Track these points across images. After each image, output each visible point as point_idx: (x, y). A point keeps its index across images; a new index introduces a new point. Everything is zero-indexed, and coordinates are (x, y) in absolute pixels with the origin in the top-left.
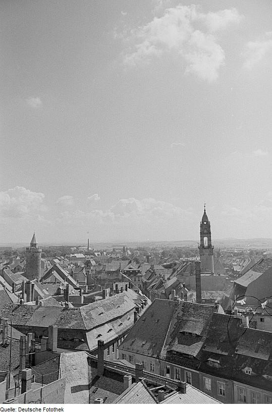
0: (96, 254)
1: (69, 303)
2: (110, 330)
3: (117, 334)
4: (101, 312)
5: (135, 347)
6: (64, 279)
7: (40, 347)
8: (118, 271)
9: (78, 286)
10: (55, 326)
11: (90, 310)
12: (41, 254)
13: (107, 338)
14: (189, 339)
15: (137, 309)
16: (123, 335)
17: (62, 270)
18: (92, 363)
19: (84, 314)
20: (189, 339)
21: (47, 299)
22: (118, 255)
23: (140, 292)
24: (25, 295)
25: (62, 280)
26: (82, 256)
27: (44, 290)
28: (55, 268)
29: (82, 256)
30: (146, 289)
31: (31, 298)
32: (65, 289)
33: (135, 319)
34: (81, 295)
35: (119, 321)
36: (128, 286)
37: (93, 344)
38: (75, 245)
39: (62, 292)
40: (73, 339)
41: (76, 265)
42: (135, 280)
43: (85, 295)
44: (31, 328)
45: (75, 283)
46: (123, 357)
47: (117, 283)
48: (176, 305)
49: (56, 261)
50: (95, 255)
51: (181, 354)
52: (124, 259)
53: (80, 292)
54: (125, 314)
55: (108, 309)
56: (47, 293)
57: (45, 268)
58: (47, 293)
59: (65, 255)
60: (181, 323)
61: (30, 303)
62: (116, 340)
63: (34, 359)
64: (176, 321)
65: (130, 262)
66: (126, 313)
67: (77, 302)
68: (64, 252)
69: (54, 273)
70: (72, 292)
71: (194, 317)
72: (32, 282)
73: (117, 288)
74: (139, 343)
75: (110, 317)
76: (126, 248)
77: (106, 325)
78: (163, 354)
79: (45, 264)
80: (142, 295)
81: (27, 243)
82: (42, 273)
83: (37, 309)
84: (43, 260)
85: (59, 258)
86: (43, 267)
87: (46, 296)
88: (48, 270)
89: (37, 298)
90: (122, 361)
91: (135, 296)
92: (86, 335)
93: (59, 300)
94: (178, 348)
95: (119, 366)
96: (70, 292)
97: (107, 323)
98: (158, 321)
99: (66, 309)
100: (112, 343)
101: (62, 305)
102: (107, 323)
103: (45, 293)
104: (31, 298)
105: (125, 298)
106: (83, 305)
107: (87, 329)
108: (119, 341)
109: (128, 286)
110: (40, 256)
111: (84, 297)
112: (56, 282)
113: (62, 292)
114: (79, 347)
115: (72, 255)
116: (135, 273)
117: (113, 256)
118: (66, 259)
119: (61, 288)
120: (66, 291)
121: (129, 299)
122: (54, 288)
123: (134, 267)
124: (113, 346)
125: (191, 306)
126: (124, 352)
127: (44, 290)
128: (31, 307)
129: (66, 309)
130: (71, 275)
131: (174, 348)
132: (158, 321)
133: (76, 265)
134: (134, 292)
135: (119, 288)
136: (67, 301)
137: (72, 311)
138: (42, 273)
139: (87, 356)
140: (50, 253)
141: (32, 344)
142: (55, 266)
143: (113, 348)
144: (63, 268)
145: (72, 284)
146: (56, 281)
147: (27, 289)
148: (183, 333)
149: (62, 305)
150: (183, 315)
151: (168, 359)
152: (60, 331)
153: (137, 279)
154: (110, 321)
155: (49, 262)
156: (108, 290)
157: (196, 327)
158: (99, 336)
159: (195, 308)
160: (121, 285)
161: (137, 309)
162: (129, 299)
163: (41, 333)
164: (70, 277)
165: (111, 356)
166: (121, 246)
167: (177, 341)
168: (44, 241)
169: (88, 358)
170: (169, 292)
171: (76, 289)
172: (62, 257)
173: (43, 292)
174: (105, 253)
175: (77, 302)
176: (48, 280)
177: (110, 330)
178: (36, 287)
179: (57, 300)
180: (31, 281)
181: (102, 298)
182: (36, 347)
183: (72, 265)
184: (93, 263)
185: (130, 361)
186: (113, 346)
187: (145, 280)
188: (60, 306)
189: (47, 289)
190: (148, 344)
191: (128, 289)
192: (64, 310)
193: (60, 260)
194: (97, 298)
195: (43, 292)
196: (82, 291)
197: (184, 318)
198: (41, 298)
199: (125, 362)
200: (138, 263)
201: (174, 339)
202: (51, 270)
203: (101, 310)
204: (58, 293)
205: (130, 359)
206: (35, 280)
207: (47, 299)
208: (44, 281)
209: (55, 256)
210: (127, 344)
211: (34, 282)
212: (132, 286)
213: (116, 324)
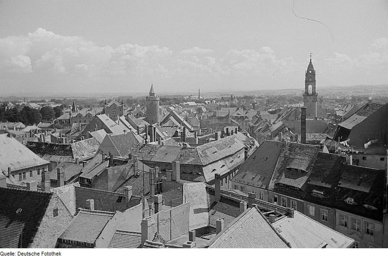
0: (206, 102)
2: (223, 166)
3: (229, 169)
4: (214, 151)
5: (246, 179)
6: (180, 123)
7: (165, 178)
8: (228, 116)
9: (192, 129)
13: (222, 172)
14: (296, 173)
15: (246, 149)
16: (235, 170)
17: (178, 116)
18: (210, 191)
20: (296, 173)
21: (168, 139)
22: (227, 103)
23: (248, 135)
24: (149, 137)
25: (178, 124)
26: (194, 103)
28: (172, 114)
29: (194, 103)
30: (253, 132)
31: (153, 139)
32: (182, 131)
33: (246, 157)
35: (231, 159)
36: (237, 129)
37: (209, 175)
40: (193, 172)
41: (189, 112)
42: (243, 125)
46: (236, 187)
47: (227, 127)
48: (284, 145)
50: (205, 103)
51: (288, 186)
52: (232, 106)
53: (195, 134)
54: (236, 153)
55: (221, 149)
56: (167, 135)
58: (167, 135)
60: (287, 160)
61: (153, 143)
62: (229, 174)
63: (161, 188)
64: (283, 159)
65: (238, 109)
66: (237, 152)
69: (172, 118)
70: (189, 135)
71: (299, 156)
73: (227, 132)
74: (250, 176)
75: (222, 155)
76: (233, 96)
77: (220, 161)
78: (272, 185)
79: (162, 111)
80: (250, 137)
81: (146, 93)
83: (160, 147)
85: (174, 106)
87: (166, 137)
89: (158, 139)
90: (235, 190)
91: (244, 138)
93: (177, 140)
94: (285, 181)
95: (233, 195)
97: (220, 160)
98: (267, 159)
99: (185, 148)
100: (225, 176)
102: (220, 160)
103: (165, 134)
104: (153, 139)
105: (236, 139)
106: (198, 145)
108: (231, 175)
109: (237, 129)
111: (199, 139)
113: (179, 134)
114: (197, 179)
115: (185, 103)
116: (242, 118)
117: (222, 103)
119: (178, 130)
120: (183, 134)
121: (239, 140)
123: (242, 113)
124: (226, 179)
125: (297, 147)
126: (237, 184)
128: (153, 147)
129: (185, 148)
131: (281, 182)
132: (267, 159)
133: (189, 112)
134: (243, 135)
135: (230, 131)
138: (160, 118)
139: (205, 186)
143: (226, 181)
144: (180, 113)
145: (188, 128)
147: (149, 131)
148: (290, 169)
150: (290, 154)
151: (275, 190)
153: (244, 123)
154: (223, 158)
155: (165, 109)
156: (219, 133)
157: (301, 163)
158: (214, 170)
159: (301, 148)
160: (231, 129)
161: (246, 149)
162: (239, 140)
163: (166, 167)
164: (185, 122)
165: (226, 187)
166: (228, 95)
167: (284, 176)
168: (159, 92)
169: (206, 188)
170: (277, 133)
173: (163, 134)
174: (214, 101)
176: (167, 124)
177: (223, 166)
178: (157, 130)
181: (214, 139)
182: (162, 178)
183: (185, 112)
184: (204, 110)
185: (242, 191)
186: (226, 179)
187: (252, 124)
188: (179, 146)
190: (259, 176)
191: (238, 132)
194: (211, 139)
195: (163, 134)
196: (197, 133)
197: (291, 157)
199: (238, 192)
200: (244, 109)
201: (281, 174)
203: (215, 149)
204: (176, 135)
205: (242, 189)
210: (239, 177)
212: (241, 130)
213: (228, 161)
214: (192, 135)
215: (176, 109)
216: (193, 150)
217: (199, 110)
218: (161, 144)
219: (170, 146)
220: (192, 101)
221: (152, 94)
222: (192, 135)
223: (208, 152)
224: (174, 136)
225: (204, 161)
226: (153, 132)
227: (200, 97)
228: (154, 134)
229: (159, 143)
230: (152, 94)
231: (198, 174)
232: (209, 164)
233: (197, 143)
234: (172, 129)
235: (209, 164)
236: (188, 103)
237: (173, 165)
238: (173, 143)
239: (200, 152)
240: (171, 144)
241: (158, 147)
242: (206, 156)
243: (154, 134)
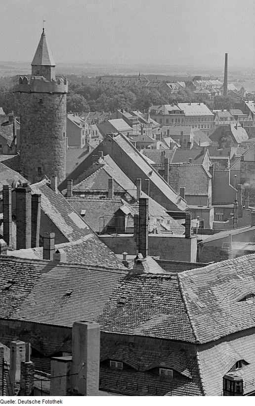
1: (149, 259)
6: (136, 182)
9: (183, 207)
10: (94, 327)
11: (212, 284)
12: (64, 100)
17: (132, 155)
19: (193, 296)
21: (79, 241)
25: (128, 185)
26: (200, 109)
27: (73, 216)
28: (109, 147)
29: (200, 109)
31: (29, 237)
34: (188, 237)
38: (180, 74)
39: (129, 223)
43: (205, 238)
44: (28, 328)
45: (173, 197)
49: (119, 124)
53: (187, 225)
56: (81, 225)
57: (82, 146)
58: (81, 225)
59: (147, 106)
67: (174, 257)
68: (147, 96)
69: (108, 163)
72: (35, 189)
82: (68, 159)
83: (47, 269)
84: (75, 118)
85: (128, 115)
86: (74, 142)
87: (78, 233)
88: (91, 151)
89: (47, 234)
92: (195, 358)
93: (117, 248)
96: (152, 225)
101: (126, 264)
103: (76, 223)
104: (29, 237)
106: (192, 266)
107: (201, 340)
110: (64, 108)
111: (200, 244)
112: (109, 191)
113: (129, 223)
115: (168, 107)
118: (150, 120)
119: (126, 209)
120: (141, 221)
122: (105, 211)
127: (73, 216)
128: (29, 265)
130: (162, 173)
136: (141, 249)
137: (153, 281)
140: (99, 96)
141: (24, 374)
142: (109, 139)
144: (138, 146)
145: (163, 200)
146: (110, 187)
149: (126, 264)
152: (109, 342)
164: (156, 179)
168: (74, 57)
171: (176, 215)
172: (139, 114)
173: (69, 222)
175: (174, 257)
176: (88, 184)
178: (46, 205)
179: (113, 249)
180: (33, 186)
183: (169, 140)
189: (83, 212)
192: (129, 278)
193: (130, 123)
195: (69, 222)
196: (195, 223)
198: (61, 238)
202: (99, 151)
204: (116, 224)
206: (44, 182)
207: (79, 241)
208: (74, 188)
209: (114, 109)
211: (37, 187)
214: (175, 229)
215: (136, 130)
216: (165, 284)
217: (222, 136)
218: (52, 259)
219: (82, 268)
220: (199, 99)
221: (41, 68)
222: (175, 229)
223: (223, 296)
224: (109, 229)
225: (202, 328)
226: (29, 213)
227: (231, 87)
228: (34, 221)
229: (46, 253)
230: (41, 68)
231: (178, 376)
232: (223, 339)
233: (193, 260)
234: (102, 203)
235: (223, 339)
236: (182, 106)
237: (75, 335)
238: (98, 255)
239: (189, 293)
240: (93, 259)
241: (38, 267)
242: (214, 309)
243: (34, 221)
